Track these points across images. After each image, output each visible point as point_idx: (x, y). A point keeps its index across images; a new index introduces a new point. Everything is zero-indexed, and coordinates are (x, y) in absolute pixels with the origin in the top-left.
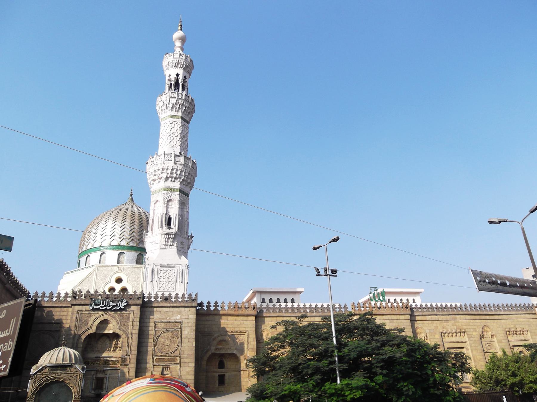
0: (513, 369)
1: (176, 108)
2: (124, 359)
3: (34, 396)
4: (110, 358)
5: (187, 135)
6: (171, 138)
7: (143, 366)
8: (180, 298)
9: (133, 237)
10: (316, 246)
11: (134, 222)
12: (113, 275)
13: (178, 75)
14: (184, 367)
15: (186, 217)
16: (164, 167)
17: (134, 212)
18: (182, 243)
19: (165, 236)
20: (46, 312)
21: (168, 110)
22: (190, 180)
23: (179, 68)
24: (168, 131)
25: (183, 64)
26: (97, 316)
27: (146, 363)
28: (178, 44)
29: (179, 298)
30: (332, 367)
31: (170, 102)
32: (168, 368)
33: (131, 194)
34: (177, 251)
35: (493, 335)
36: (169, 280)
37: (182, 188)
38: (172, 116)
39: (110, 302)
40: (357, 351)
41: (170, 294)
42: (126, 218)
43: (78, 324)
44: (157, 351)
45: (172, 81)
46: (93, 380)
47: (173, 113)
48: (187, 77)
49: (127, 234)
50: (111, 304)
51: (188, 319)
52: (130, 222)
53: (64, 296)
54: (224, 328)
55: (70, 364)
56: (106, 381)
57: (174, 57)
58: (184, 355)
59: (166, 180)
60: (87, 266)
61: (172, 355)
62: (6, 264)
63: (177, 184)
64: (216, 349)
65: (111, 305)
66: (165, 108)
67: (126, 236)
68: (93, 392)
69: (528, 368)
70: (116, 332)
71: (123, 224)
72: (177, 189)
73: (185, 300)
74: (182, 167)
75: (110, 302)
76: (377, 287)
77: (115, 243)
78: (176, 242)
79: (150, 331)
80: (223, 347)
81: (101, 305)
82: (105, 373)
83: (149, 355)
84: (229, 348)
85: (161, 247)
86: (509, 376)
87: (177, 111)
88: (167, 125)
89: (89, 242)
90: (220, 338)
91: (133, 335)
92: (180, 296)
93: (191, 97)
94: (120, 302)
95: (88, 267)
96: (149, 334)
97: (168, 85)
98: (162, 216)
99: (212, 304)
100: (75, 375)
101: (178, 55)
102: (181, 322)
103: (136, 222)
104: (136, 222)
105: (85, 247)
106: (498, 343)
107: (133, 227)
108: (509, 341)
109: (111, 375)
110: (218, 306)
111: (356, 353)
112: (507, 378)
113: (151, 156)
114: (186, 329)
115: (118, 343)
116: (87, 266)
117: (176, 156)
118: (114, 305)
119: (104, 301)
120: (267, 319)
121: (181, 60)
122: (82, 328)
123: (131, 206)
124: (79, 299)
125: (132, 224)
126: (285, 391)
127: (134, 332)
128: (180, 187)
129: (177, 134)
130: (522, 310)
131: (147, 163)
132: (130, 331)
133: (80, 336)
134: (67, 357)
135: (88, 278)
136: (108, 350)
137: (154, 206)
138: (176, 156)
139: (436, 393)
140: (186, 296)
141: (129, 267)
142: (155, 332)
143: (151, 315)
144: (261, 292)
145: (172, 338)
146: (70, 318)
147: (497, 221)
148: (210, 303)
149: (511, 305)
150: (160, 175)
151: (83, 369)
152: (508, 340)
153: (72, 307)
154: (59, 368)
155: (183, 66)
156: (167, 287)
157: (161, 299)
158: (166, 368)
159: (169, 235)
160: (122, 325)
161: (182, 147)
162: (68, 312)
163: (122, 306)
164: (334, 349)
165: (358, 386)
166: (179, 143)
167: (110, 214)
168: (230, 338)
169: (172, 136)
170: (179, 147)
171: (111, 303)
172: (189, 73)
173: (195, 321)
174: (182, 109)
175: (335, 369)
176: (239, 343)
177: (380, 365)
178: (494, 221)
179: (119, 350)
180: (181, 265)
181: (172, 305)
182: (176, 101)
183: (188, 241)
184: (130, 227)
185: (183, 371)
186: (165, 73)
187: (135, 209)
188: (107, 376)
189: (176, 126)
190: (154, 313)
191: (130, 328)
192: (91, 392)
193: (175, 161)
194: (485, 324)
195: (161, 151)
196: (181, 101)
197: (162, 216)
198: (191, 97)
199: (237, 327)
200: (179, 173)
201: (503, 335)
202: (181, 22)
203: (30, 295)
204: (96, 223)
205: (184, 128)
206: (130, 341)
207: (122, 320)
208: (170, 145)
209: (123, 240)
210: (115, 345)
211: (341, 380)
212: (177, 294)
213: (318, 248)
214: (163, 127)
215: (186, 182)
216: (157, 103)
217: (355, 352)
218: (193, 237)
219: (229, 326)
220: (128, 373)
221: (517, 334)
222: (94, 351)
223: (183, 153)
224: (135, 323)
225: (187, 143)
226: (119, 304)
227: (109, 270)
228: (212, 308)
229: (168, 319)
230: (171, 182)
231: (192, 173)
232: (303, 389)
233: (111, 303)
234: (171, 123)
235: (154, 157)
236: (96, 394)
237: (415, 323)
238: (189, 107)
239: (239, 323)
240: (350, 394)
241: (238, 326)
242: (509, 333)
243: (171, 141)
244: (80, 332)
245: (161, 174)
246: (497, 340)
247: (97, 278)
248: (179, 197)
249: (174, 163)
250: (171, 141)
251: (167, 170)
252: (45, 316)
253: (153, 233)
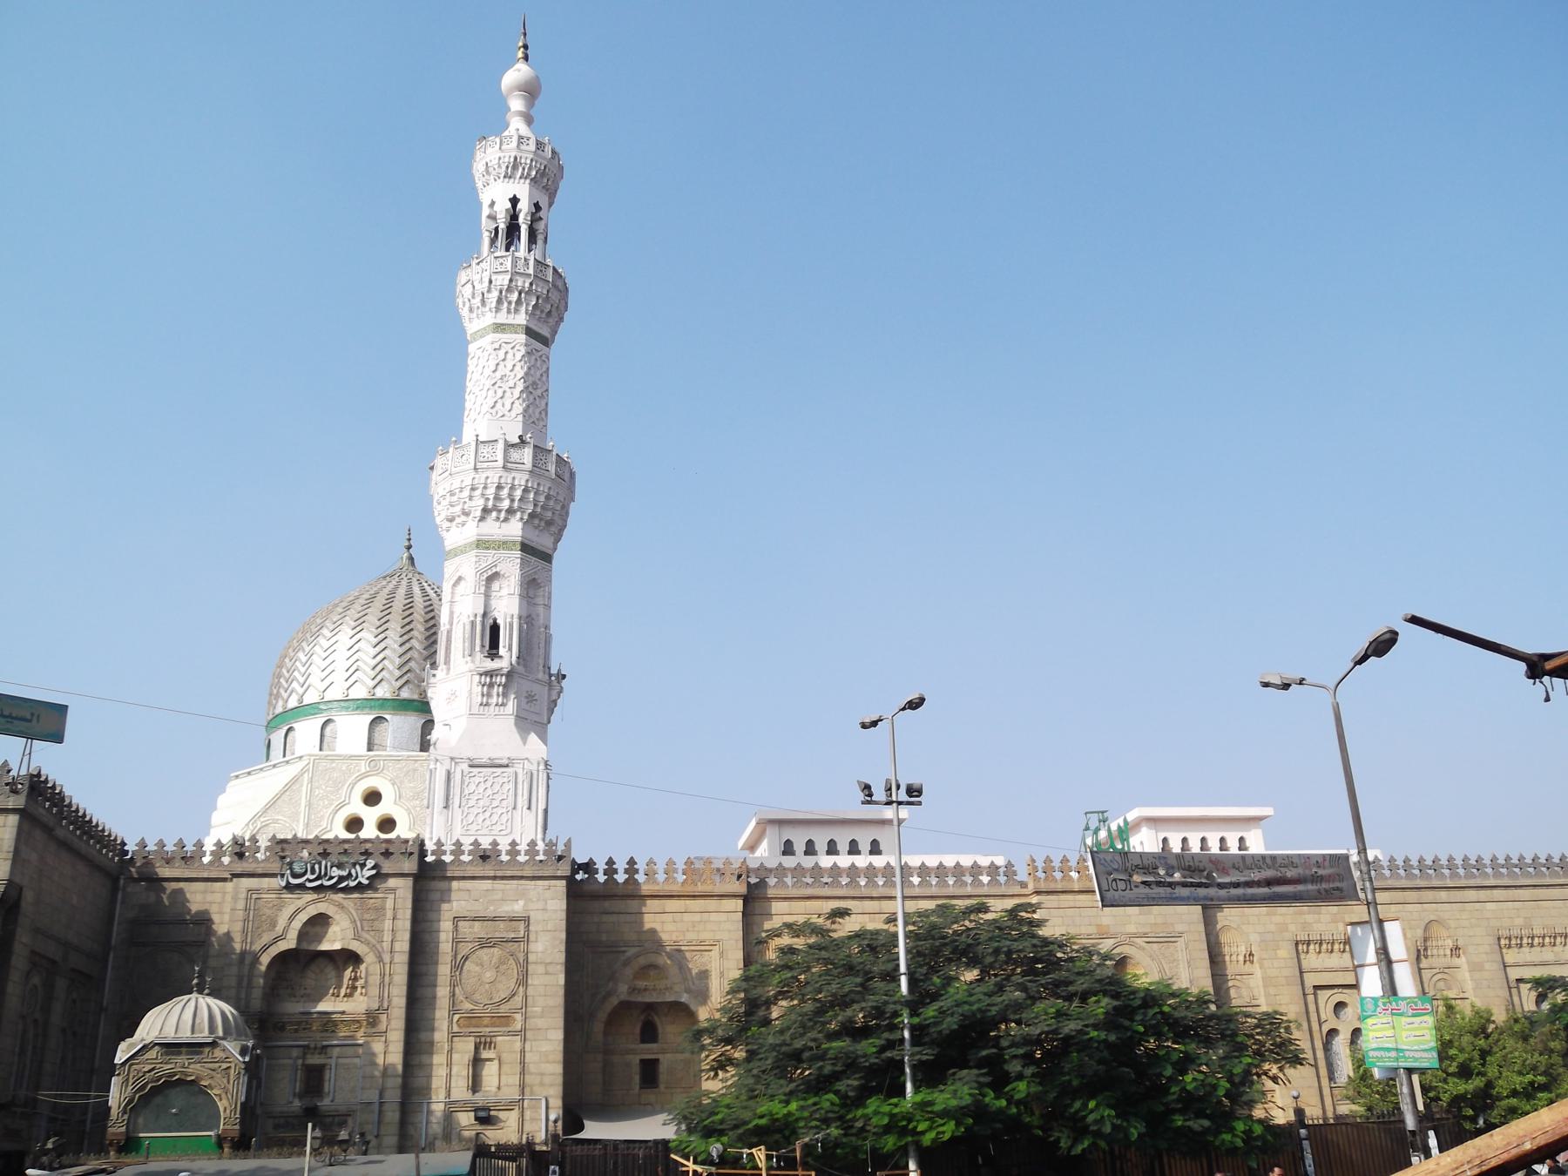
0: (1462, 1058)
1: (510, 303)
2: (372, 1018)
3: (126, 1117)
4: (339, 1015)
5: (544, 378)
6: (495, 393)
7: (423, 1036)
8: (523, 853)
9: (409, 675)
10: (867, 720)
11: (412, 630)
12: (356, 783)
13: (514, 201)
14: (535, 1040)
15: (541, 621)
16: (476, 481)
17: (412, 602)
18: (530, 698)
19: (481, 678)
20: (168, 892)
21: (487, 309)
22: (553, 513)
23: (517, 181)
24: (488, 372)
25: (530, 169)
26: (300, 903)
27: (433, 1030)
28: (517, 104)
29: (518, 853)
30: (890, 1055)
31: (492, 286)
32: (491, 1043)
33: (407, 544)
34: (516, 720)
35: (1457, 948)
36: (495, 803)
37: (529, 536)
38: (499, 328)
39: (331, 867)
40: (962, 1015)
41: (495, 844)
42: (388, 621)
43: (250, 926)
44: (461, 998)
45: (498, 221)
46: (297, 1070)
47: (503, 318)
48: (544, 204)
49: (392, 666)
50: (336, 872)
51: (545, 910)
52: (399, 629)
53: (212, 853)
54: (653, 932)
55: (210, 1040)
56: (330, 1073)
57: (503, 147)
58: (535, 1009)
59: (482, 519)
60: (287, 759)
61: (504, 1008)
62: (49, 779)
63: (515, 529)
64: (633, 990)
65: (333, 875)
66: (479, 305)
67: (391, 673)
68: (297, 1103)
69: (1511, 1052)
70: (350, 948)
71: (380, 636)
72: (514, 543)
73: (538, 858)
74: (527, 477)
75: (331, 867)
76: (1106, 811)
77: (360, 692)
78: (513, 696)
79: (440, 945)
80: (653, 984)
81: (309, 876)
82: (326, 1053)
83: (440, 1009)
84: (667, 989)
85: (470, 710)
86: (1448, 1074)
87: (512, 311)
88: (486, 354)
89: (290, 688)
90: (642, 961)
91: (396, 955)
92: (523, 847)
93: (554, 267)
94: (358, 867)
95: (287, 762)
96: (440, 951)
97: (487, 234)
98: (472, 622)
99: (621, 865)
100: (225, 1066)
101: (515, 139)
102: (527, 920)
103: (418, 630)
104: (418, 630)
105: (280, 703)
106: (1470, 971)
107: (407, 646)
108: (1505, 967)
109: (341, 1061)
110: (637, 871)
111: (956, 1018)
112: (1445, 1081)
113: (441, 448)
114: (539, 939)
115: (358, 975)
116: (287, 759)
117: (509, 446)
119: (314, 864)
120: (776, 907)
121: (524, 155)
122: (260, 936)
123: (404, 582)
124: (251, 860)
125: (406, 637)
126: (761, 1117)
127: (397, 947)
128: (522, 537)
129: (514, 381)
130: (1556, 875)
131: (432, 468)
132: (386, 945)
133: (256, 959)
134: (203, 1021)
135: (288, 793)
136: (333, 995)
137: (453, 593)
138: (509, 446)
139: (1189, 1127)
140: (541, 846)
141: (400, 758)
142: (456, 948)
143: (443, 901)
144: (781, 823)
145: (502, 962)
146: (228, 910)
147: (1280, 683)
148: (614, 863)
149: (1521, 858)
150: (465, 502)
151: (243, 1052)
152: (1504, 963)
153: (235, 880)
154: (184, 1050)
155: (529, 174)
156: (488, 822)
157: (471, 858)
158: (485, 1043)
159: (491, 676)
160: (366, 929)
161: (530, 416)
162: (224, 893)
163: (363, 876)
164: (898, 1007)
165: (948, 1108)
166: (519, 408)
167: (347, 609)
168: (672, 960)
170: (520, 418)
171: (334, 869)
172: (550, 191)
173: (563, 915)
174: (527, 305)
175: (902, 1062)
176: (694, 972)
177: (1021, 1051)
178: (1272, 682)
179: (362, 994)
180: (526, 761)
181: (499, 874)
182: (507, 283)
183: (550, 690)
184: (401, 645)
185: (531, 1051)
186: (480, 194)
187: (416, 590)
188: (333, 1062)
189: (510, 356)
190: (453, 894)
191: (387, 937)
192: (291, 1103)
193: (506, 460)
194: (1433, 918)
195: (468, 436)
196: (524, 282)
197: (473, 623)
198: (554, 267)
199: (690, 929)
200: (519, 497)
201: (1487, 948)
202: (525, 34)
203: (126, 848)
204: (308, 635)
205: (536, 359)
206: (387, 972)
207: (367, 916)
208: (494, 414)
209: (383, 683)
210: (350, 979)
211: (917, 1089)
212: (514, 844)
213: (874, 724)
214: (475, 359)
215: (541, 520)
216: (459, 288)
217: (955, 1016)
218: (564, 677)
219: (670, 927)
220: (383, 1055)
221: (1532, 945)
222: (295, 996)
223: (529, 435)
224: (399, 923)
225: (543, 403)
226: (357, 873)
227: (344, 768)
228: (621, 877)
229: (491, 911)
230: (498, 524)
231: (558, 493)
232: (806, 1114)
233: (334, 869)
234: (495, 349)
235: (448, 452)
236: (304, 1107)
237: (1219, 914)
238: (548, 297)
239: (697, 917)
240: (930, 1128)
241: (694, 926)
242: (1504, 942)
243: (496, 402)
244: (257, 947)
245: (467, 500)
246: (1468, 962)
247: (313, 791)
248: (519, 565)
249: (504, 467)
250: (496, 402)
251: (485, 488)
252: (167, 903)
253: (449, 669)
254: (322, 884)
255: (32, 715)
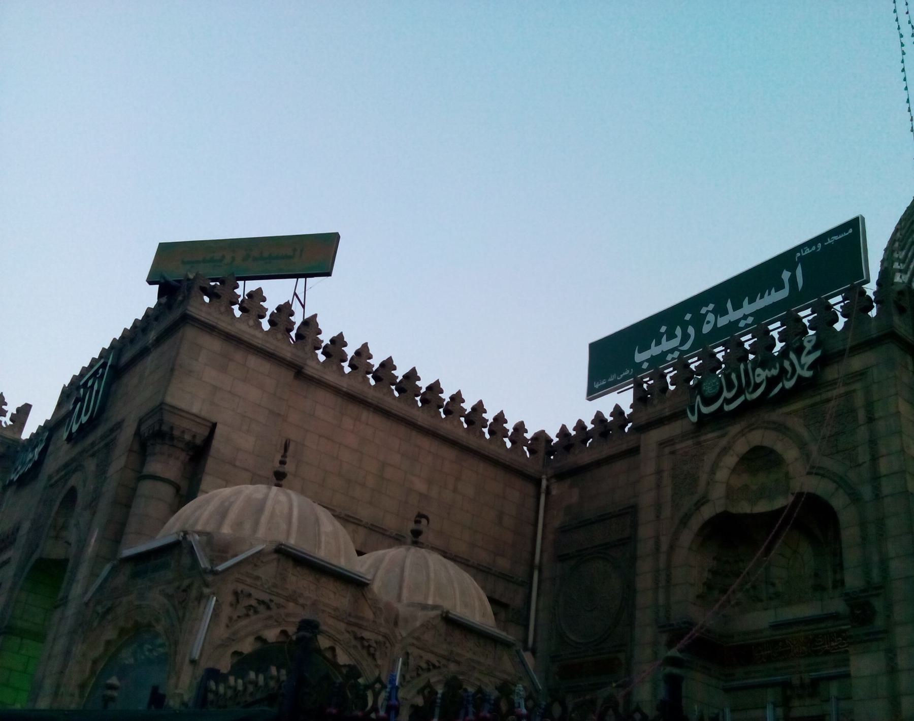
50: (761, 375)
65: (758, 380)
75: (754, 370)
81: (726, 394)
94: (792, 356)
118: (773, 377)
163: (802, 367)
171: (759, 371)
191: (863, 456)
226: (792, 365)
254: (746, 400)
255: (295, 250)
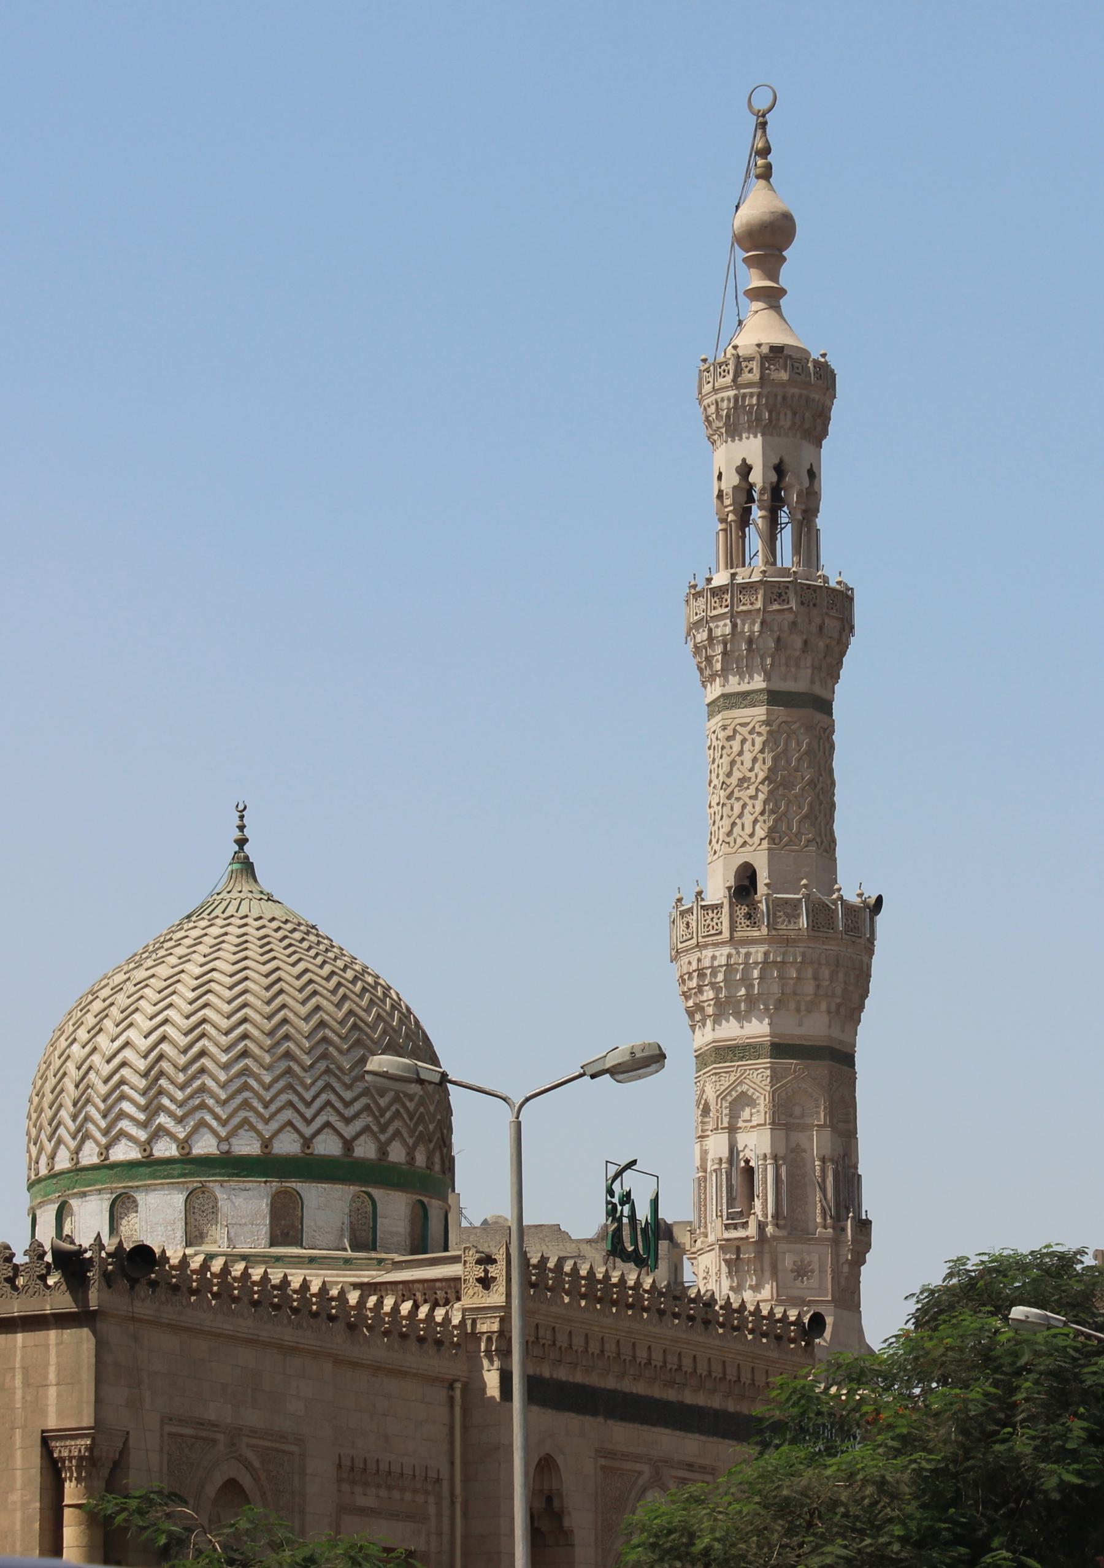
38: (730, 701)
47: (734, 685)
155: (759, 419)
169: (738, 799)
170: (765, 844)
197: (702, 1182)
208: (732, 844)
